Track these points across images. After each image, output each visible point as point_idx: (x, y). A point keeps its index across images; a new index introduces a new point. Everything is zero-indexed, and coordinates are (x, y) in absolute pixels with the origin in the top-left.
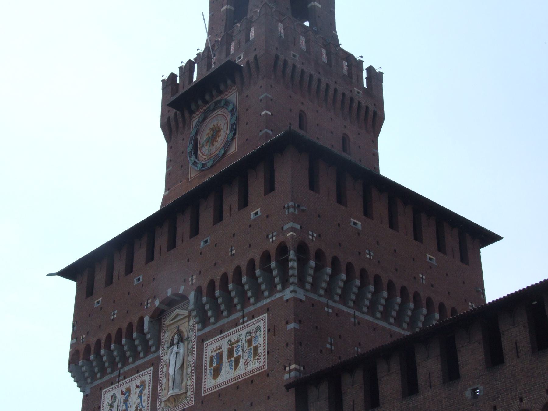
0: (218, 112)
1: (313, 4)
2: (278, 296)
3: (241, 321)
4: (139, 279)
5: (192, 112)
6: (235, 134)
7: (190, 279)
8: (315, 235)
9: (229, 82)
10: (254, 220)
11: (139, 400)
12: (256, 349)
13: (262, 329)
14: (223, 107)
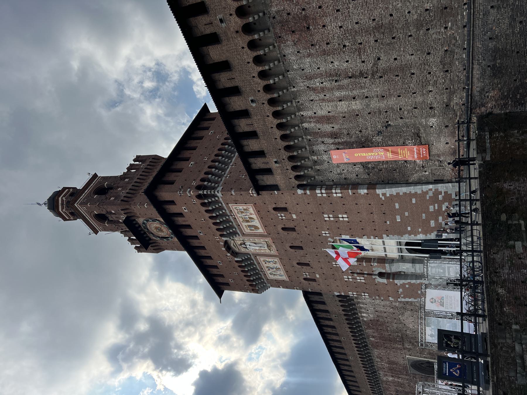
0: (148, 227)
1: (105, 186)
2: (221, 199)
3: (233, 216)
4: (220, 263)
5: (150, 239)
6: (157, 220)
7: (217, 239)
8: (194, 182)
9: (134, 222)
10: (188, 210)
11: (271, 262)
12: (244, 209)
13: (236, 207)
14: (146, 225)
